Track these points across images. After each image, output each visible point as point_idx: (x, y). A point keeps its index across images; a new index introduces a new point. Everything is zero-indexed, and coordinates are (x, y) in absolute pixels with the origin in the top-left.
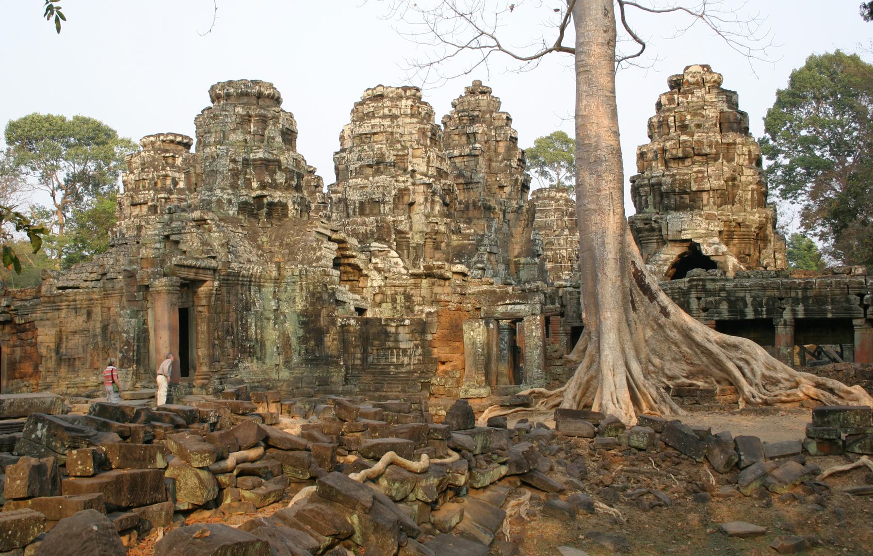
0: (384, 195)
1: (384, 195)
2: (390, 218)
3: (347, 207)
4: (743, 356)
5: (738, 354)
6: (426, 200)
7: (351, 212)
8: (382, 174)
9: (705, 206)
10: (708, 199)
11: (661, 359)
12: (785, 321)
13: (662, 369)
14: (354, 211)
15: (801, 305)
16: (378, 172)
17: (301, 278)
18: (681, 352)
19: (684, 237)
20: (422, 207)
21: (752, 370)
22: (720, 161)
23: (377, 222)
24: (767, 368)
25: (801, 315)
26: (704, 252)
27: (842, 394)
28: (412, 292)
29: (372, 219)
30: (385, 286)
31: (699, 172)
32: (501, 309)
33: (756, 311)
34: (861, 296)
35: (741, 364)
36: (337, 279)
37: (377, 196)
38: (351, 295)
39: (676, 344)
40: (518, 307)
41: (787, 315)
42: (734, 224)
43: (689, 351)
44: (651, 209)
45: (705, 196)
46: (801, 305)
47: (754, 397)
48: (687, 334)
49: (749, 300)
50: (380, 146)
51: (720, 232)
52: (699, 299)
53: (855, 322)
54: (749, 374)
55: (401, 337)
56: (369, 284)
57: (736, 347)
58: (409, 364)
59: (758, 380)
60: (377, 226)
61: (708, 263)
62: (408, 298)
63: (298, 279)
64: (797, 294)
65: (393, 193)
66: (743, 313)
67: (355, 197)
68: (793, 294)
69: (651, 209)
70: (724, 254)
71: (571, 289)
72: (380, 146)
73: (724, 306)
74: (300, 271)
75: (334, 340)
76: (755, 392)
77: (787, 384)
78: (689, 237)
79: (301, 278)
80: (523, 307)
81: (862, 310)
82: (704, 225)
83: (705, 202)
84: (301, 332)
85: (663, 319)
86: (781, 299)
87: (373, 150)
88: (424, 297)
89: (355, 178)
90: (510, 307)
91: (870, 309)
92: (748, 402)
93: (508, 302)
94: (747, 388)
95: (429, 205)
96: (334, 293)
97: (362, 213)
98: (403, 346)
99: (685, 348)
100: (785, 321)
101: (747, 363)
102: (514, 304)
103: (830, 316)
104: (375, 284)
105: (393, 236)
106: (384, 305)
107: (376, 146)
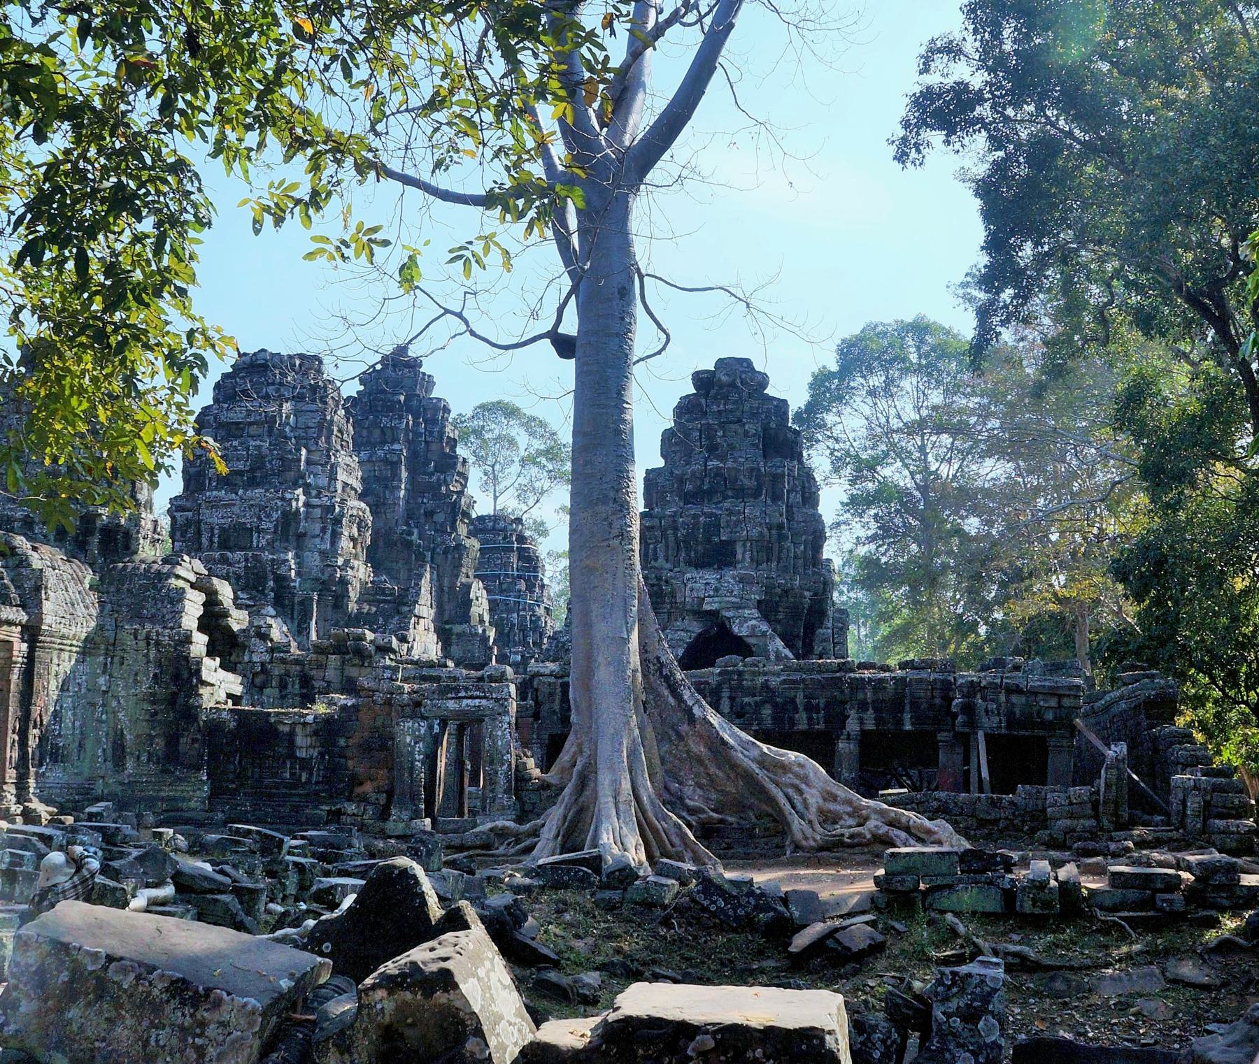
0: (260, 519)
1: (260, 519)
2: (267, 556)
3: (199, 533)
6: (323, 530)
7: (205, 541)
8: (258, 485)
10: (744, 553)
11: (680, 783)
12: (849, 734)
13: (681, 799)
14: (211, 542)
16: (253, 483)
17: (148, 644)
18: (708, 774)
19: (706, 607)
20: (317, 541)
21: (805, 800)
23: (246, 560)
25: (870, 725)
27: (923, 836)
28: (314, 673)
29: (238, 555)
30: (271, 662)
32: (451, 704)
33: (810, 719)
35: (790, 791)
36: (204, 650)
37: (248, 520)
38: (222, 673)
39: (700, 761)
40: (477, 702)
41: (852, 725)
42: (778, 590)
43: (720, 774)
44: (661, 562)
45: (739, 550)
47: (806, 839)
48: (718, 747)
49: (800, 699)
50: (258, 443)
51: (759, 602)
52: (732, 699)
53: (942, 736)
54: (800, 807)
55: (300, 740)
56: (246, 658)
58: (309, 781)
59: (813, 816)
60: (246, 567)
61: (741, 647)
62: (306, 681)
63: (142, 644)
65: (275, 516)
66: (793, 723)
67: (214, 518)
68: (860, 696)
69: (661, 562)
70: (764, 634)
71: (552, 680)
72: (258, 443)
73: (767, 711)
74: (148, 633)
75: (194, 741)
76: (809, 832)
77: (851, 822)
78: (715, 607)
79: (148, 644)
80: (484, 702)
81: (949, 720)
83: (739, 557)
84: (143, 728)
85: (685, 728)
86: (843, 703)
87: (248, 449)
88: (329, 683)
89: (216, 488)
90: (465, 702)
91: (960, 719)
92: (797, 847)
93: (462, 694)
94: (797, 824)
95: (328, 536)
96: (198, 671)
97: (224, 545)
98: (301, 754)
99: (713, 770)
100: (849, 734)
101: (800, 792)
102: (472, 697)
104: (256, 658)
105: (271, 583)
106: (267, 691)
107: (252, 443)
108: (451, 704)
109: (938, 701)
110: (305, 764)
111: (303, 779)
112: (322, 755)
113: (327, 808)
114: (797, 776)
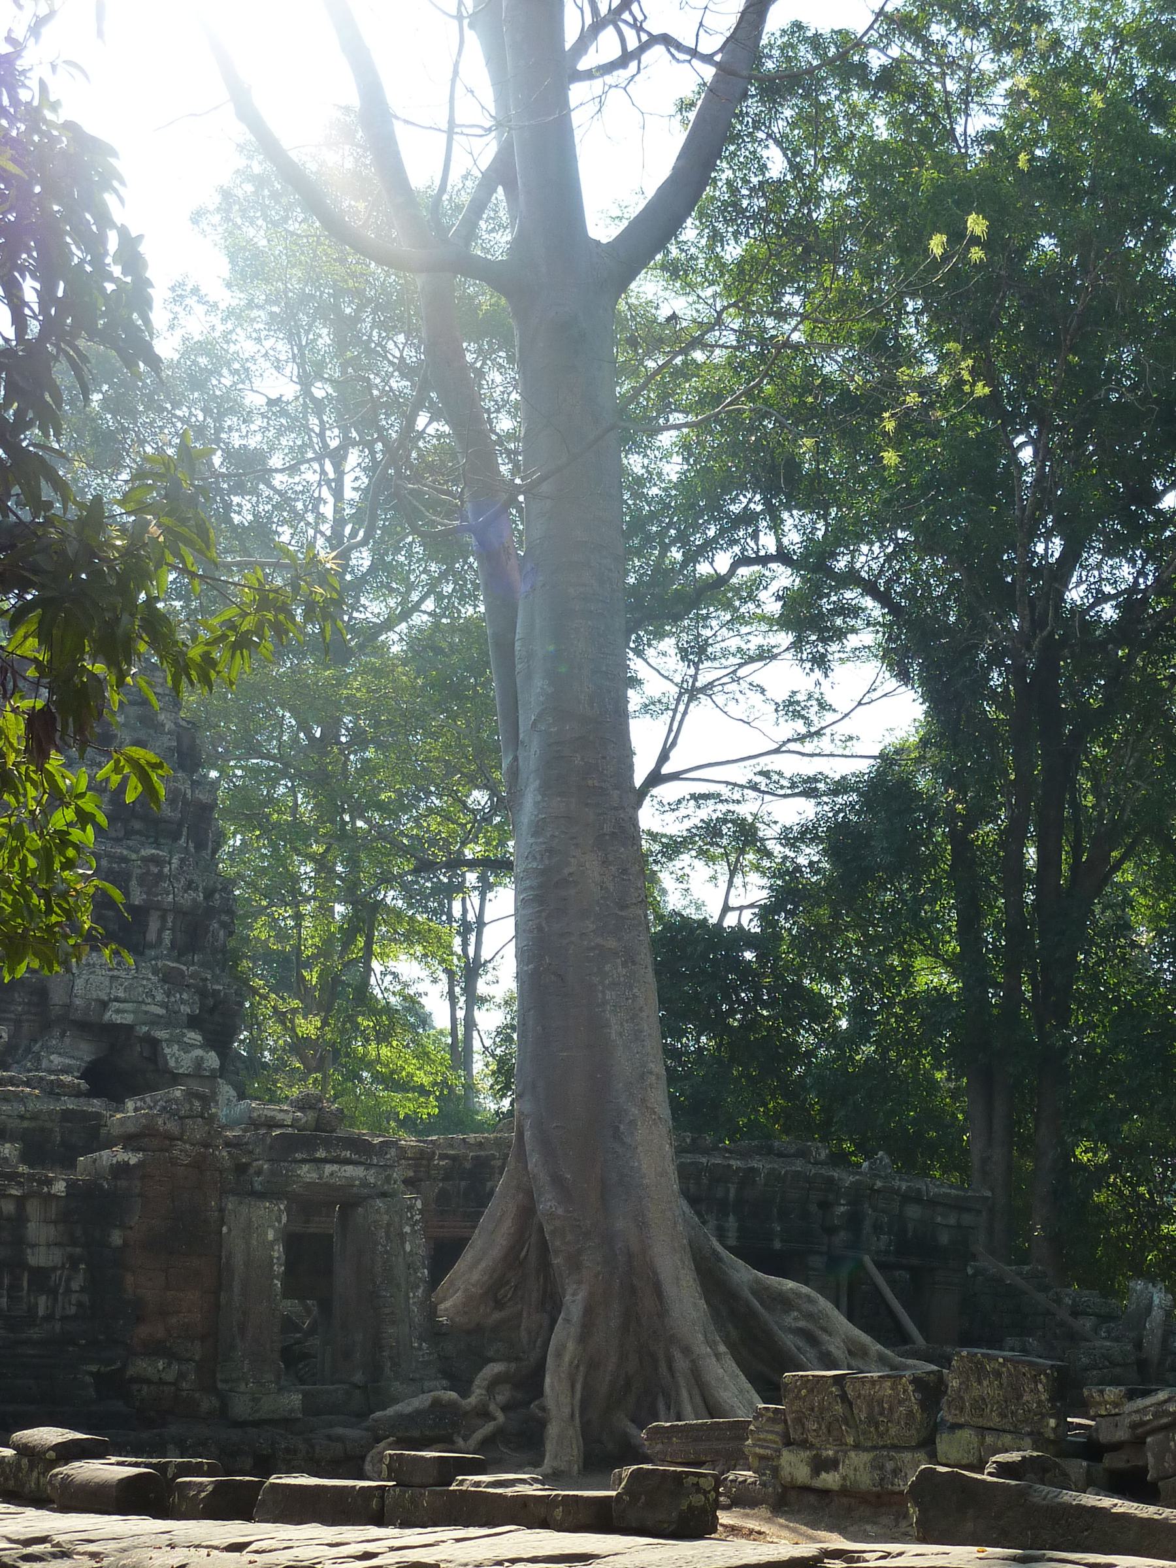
4: (802, 1324)
5: (791, 1320)
9: (152, 946)
15: (731, 1218)
22: (182, 841)
24: (850, 1352)
26: (172, 1063)
31: (153, 859)
32: (306, 1172)
34: (825, 1206)
40: (349, 1171)
42: (211, 1002)
45: (154, 925)
46: (731, 1218)
57: (784, 1302)
58: (49, 1317)
64: (728, 1191)
78: (128, 1019)
80: (359, 1172)
82: (160, 997)
90: (329, 1168)
91: (843, 1235)
98: (38, 1258)
103: (777, 1245)
108: (306, 1172)
109: (813, 1208)
110: (40, 1276)
111: (41, 1312)
112: (74, 1262)
113: (94, 1368)
114: (809, 1316)
